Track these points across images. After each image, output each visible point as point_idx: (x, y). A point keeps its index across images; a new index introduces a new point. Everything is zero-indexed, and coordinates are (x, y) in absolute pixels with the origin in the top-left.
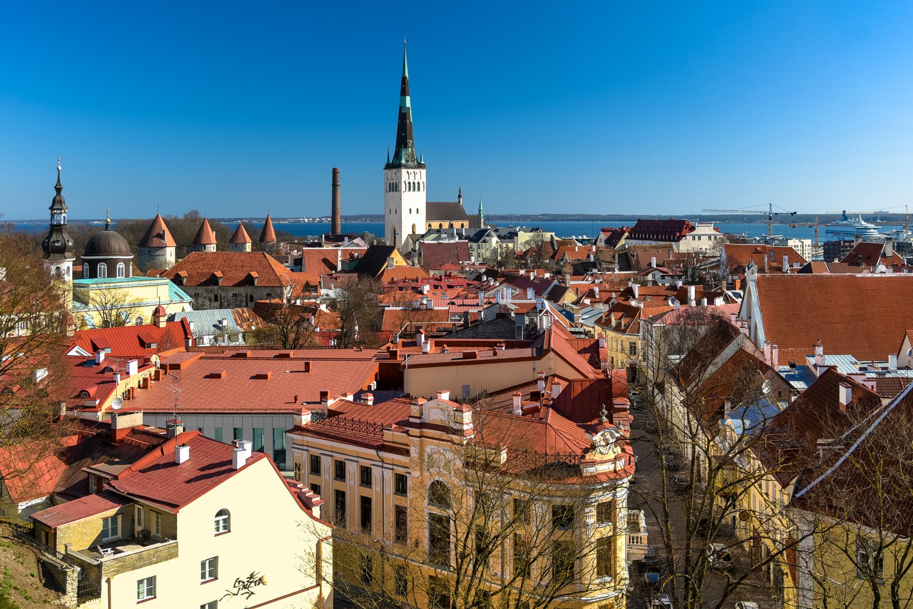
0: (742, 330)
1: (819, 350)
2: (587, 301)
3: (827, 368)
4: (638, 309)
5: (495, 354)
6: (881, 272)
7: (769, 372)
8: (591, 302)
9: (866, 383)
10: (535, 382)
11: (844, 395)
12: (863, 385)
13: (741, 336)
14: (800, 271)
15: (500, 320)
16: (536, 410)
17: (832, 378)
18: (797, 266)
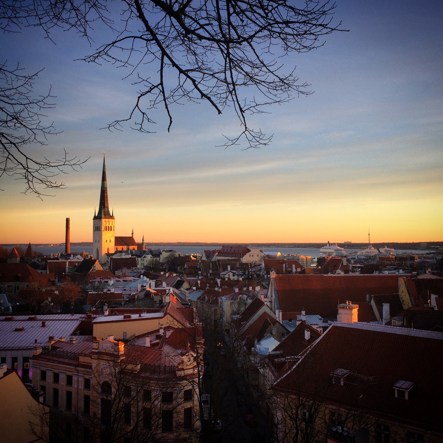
0: (265, 303)
1: (303, 312)
2: (194, 288)
3: (300, 322)
4: (218, 292)
5: (140, 316)
6: (339, 274)
7: (277, 324)
8: (196, 289)
9: (318, 329)
10: (158, 331)
11: (307, 335)
12: (316, 330)
13: (265, 306)
14: (300, 273)
15: (146, 298)
16: (157, 344)
17: (304, 326)
18: (299, 270)
